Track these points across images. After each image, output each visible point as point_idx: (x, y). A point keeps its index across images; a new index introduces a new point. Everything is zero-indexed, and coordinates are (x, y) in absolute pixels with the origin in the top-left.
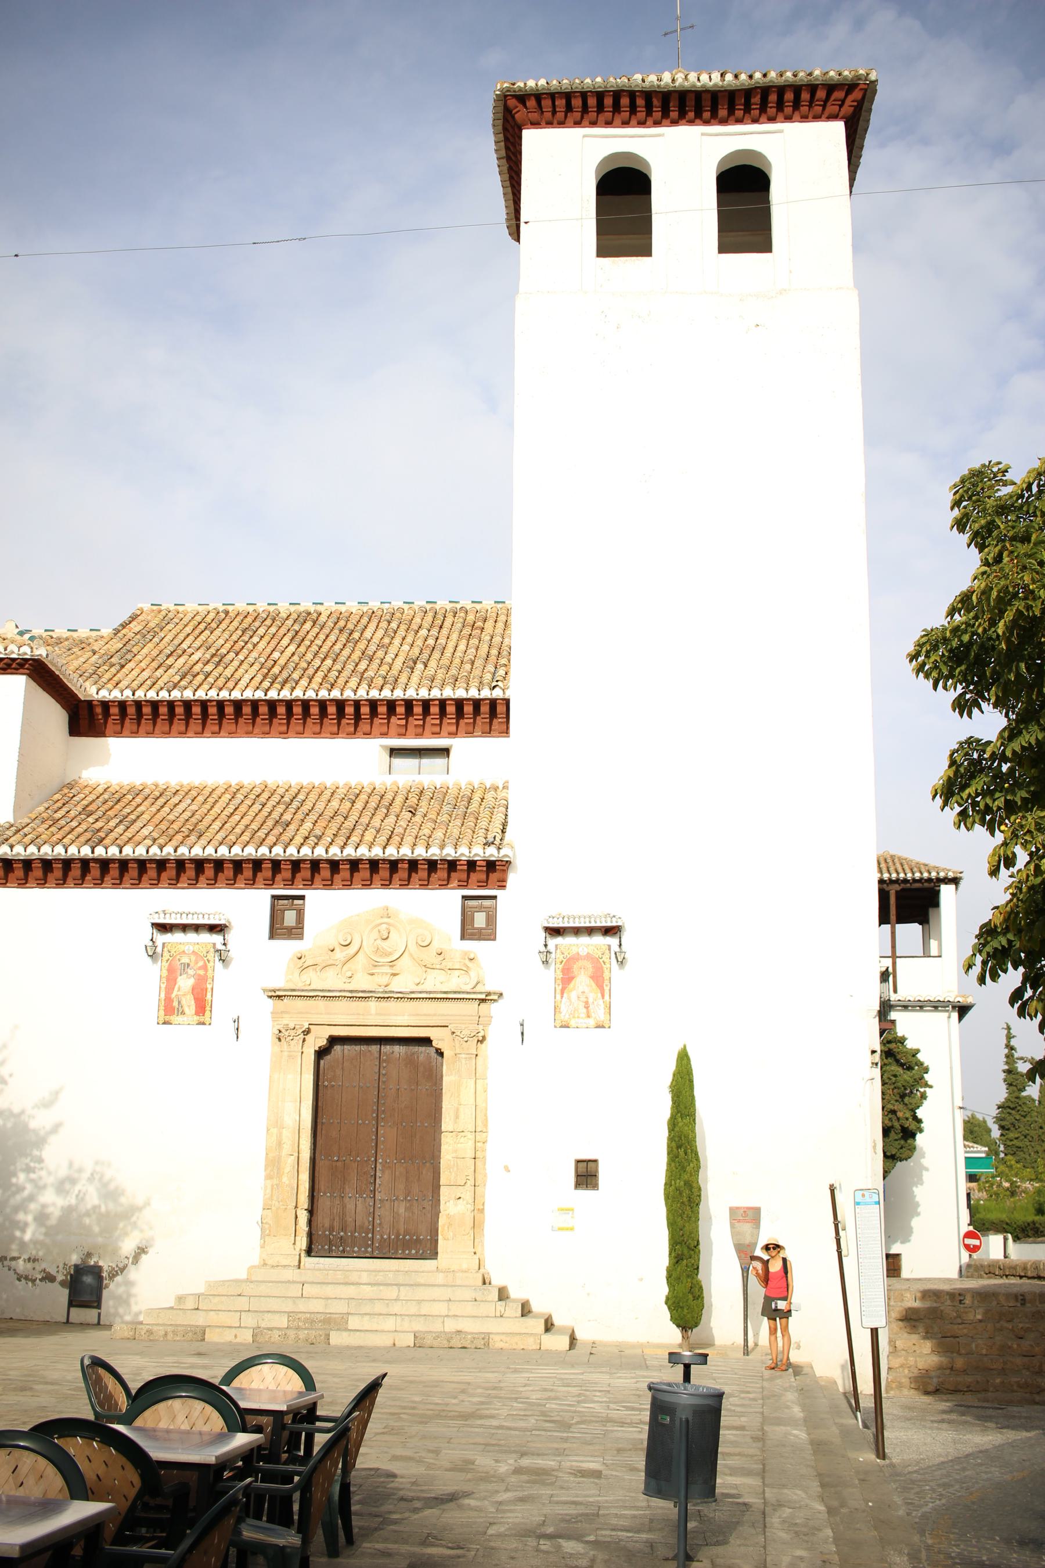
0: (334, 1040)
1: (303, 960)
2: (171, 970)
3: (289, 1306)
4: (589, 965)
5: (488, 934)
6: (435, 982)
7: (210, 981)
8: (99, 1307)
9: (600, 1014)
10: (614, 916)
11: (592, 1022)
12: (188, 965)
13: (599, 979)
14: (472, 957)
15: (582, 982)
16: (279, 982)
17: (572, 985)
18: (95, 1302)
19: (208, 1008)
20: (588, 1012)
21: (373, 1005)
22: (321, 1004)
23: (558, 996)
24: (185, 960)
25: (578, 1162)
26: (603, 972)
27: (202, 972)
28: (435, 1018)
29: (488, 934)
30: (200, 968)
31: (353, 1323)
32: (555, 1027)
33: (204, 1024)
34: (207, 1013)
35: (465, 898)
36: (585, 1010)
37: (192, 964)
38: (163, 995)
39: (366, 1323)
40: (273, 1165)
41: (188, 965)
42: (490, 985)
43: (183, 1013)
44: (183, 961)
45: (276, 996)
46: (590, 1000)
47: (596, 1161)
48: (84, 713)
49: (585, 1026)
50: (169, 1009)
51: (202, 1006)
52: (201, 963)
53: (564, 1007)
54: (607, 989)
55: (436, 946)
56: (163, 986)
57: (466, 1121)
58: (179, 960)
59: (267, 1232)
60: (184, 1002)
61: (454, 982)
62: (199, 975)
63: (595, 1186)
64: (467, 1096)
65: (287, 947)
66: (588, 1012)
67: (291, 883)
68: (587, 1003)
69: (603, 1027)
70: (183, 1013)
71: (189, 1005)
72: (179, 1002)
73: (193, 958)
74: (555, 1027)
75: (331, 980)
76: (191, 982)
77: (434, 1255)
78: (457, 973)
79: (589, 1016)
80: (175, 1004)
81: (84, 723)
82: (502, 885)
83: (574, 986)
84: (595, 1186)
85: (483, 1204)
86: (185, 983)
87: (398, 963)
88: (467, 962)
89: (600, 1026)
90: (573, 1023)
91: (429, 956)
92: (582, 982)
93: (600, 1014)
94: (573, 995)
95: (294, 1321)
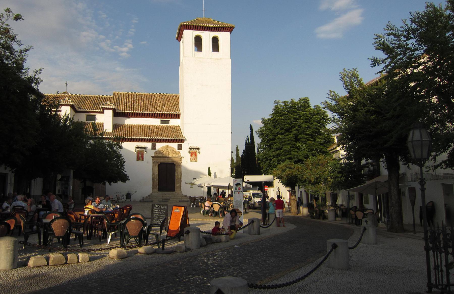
0: (161, 163)
5: (181, 149)
8: (130, 198)
9: (196, 160)
13: (196, 155)
15: (194, 156)
16: (153, 155)
18: (130, 198)
29: (181, 149)
40: (153, 180)
45: (153, 157)
51: (143, 159)
57: (179, 173)
59: (153, 188)
65: (155, 151)
67: (155, 142)
71: (141, 159)
77: (174, 191)
86: (140, 155)
89: (196, 161)
92: (194, 156)
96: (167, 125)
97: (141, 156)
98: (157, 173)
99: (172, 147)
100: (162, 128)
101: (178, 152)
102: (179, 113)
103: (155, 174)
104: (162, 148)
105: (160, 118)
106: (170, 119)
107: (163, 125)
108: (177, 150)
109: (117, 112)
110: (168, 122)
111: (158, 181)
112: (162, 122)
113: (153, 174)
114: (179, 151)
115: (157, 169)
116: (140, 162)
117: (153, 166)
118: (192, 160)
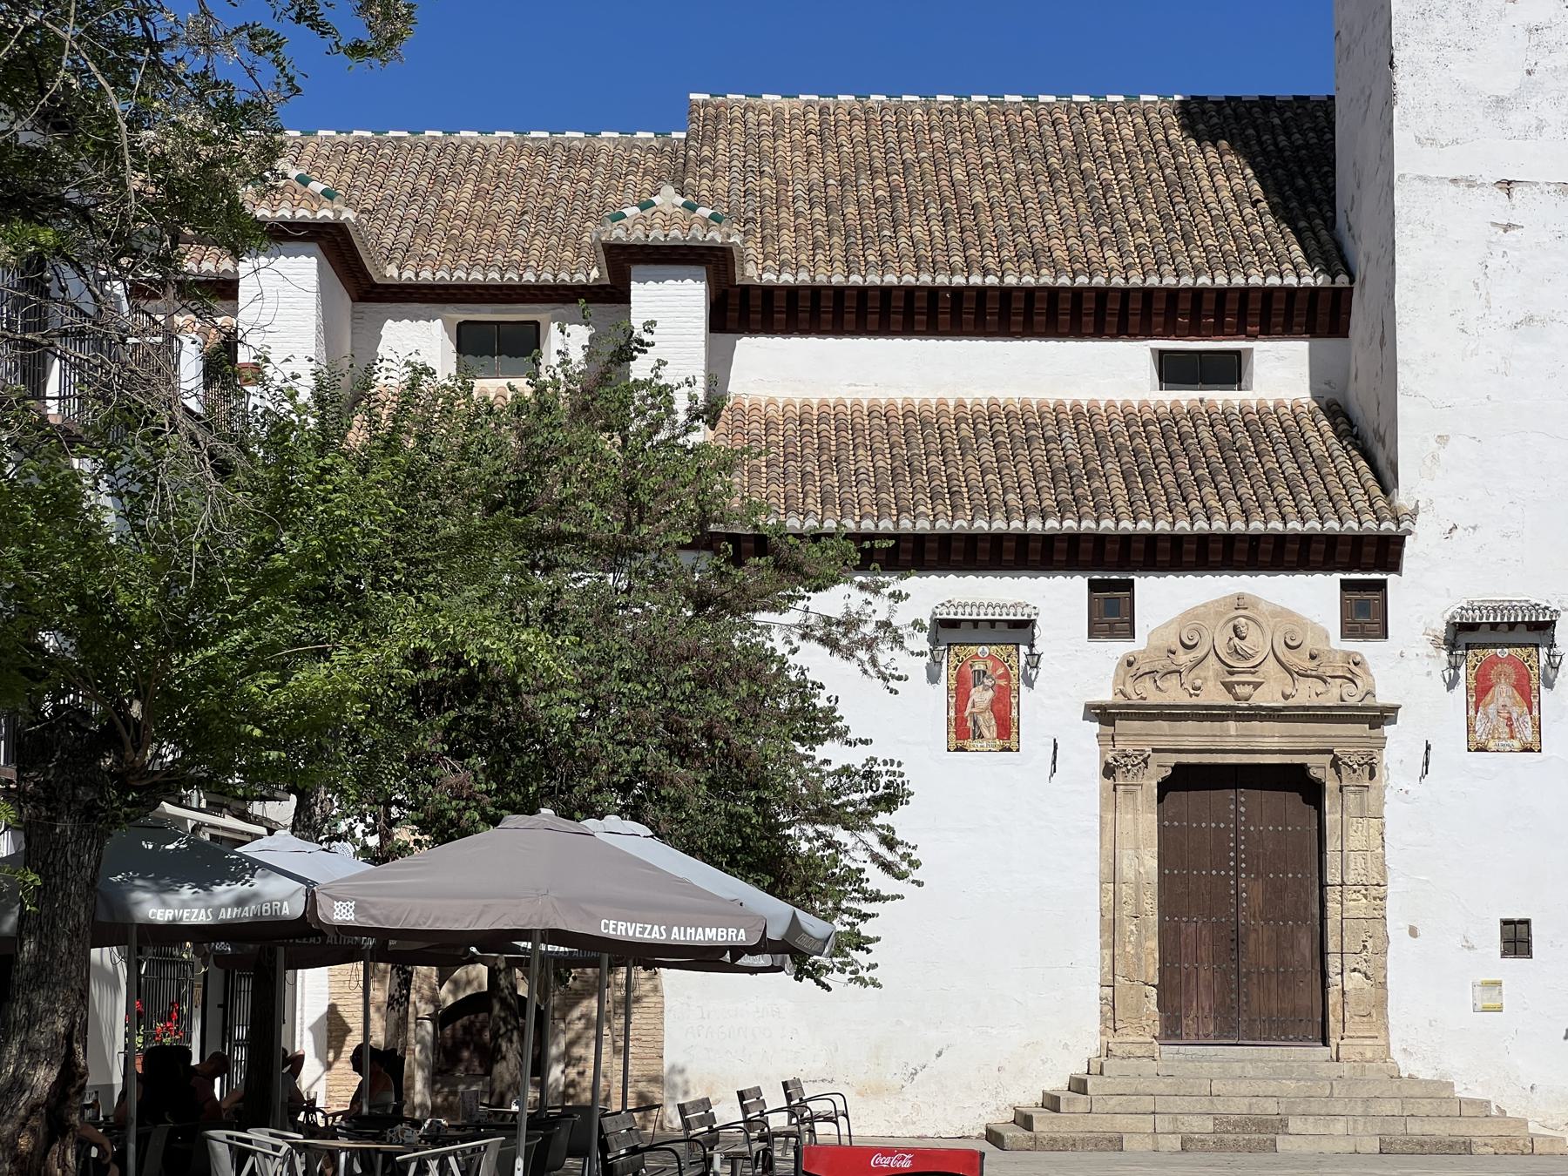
1: (1135, 666)
2: (961, 679)
3: (1205, 1104)
4: (1509, 669)
6: (1306, 694)
7: (1014, 693)
9: (1528, 734)
10: (1547, 608)
11: (1516, 744)
12: (985, 673)
13: (1526, 693)
14: (1358, 659)
15: (1503, 693)
16: (1106, 696)
17: (1488, 698)
19: (1014, 730)
20: (1511, 731)
21: (1232, 726)
22: (1165, 725)
23: (1472, 712)
24: (979, 666)
25: (1505, 923)
26: (1530, 679)
27: (1003, 683)
28: (1314, 739)
30: (1000, 677)
31: (1295, 1125)
32: (1469, 750)
33: (1010, 750)
34: (1014, 736)
35: (1346, 586)
36: (1507, 729)
37: (989, 673)
38: (952, 714)
39: (1310, 1126)
40: (1111, 929)
41: (985, 673)
42: (1383, 698)
43: (981, 736)
44: (976, 668)
45: (1102, 714)
46: (1515, 716)
47: (1527, 922)
48: (734, 301)
49: (1508, 748)
50: (962, 733)
51: (1006, 729)
52: (1001, 671)
53: (1479, 727)
54: (1535, 701)
55: (1309, 645)
56: (952, 701)
58: (971, 666)
59: (1111, 1017)
60: (981, 722)
61: (1331, 696)
62: (1000, 686)
63: (1528, 953)
64: (1355, 840)
65: (1119, 649)
66: (1511, 731)
68: (1510, 719)
69: (1531, 750)
70: (981, 736)
71: (989, 728)
72: (975, 723)
73: (990, 663)
74: (1469, 750)
75: (1173, 693)
76: (990, 694)
78: (1339, 681)
79: (1512, 737)
80: (970, 724)
81: (733, 315)
82: (1394, 566)
83: (1492, 698)
84: (1528, 953)
85: (1385, 977)
86: (981, 697)
87: (1261, 669)
88: (1352, 666)
90: (1491, 745)
91: (1299, 660)
92: (1503, 693)
93: (1528, 734)
94: (1492, 709)
95: (1222, 1123)
96: (1218, 397)
97: (993, 702)
98: (1144, 862)
99: (1282, 614)
100: (1170, 427)
101: (1348, 655)
102: (1342, 280)
103: (1127, 869)
104: (1194, 618)
105: (1165, 335)
106: (1252, 337)
107: (1186, 397)
108: (1337, 643)
109: (746, 290)
110: (1229, 371)
111: (1153, 944)
112: (1173, 371)
113: (1112, 876)
114: (1354, 646)
115: (1142, 821)
116: (982, 763)
117: (1110, 803)
118: (1492, 734)
